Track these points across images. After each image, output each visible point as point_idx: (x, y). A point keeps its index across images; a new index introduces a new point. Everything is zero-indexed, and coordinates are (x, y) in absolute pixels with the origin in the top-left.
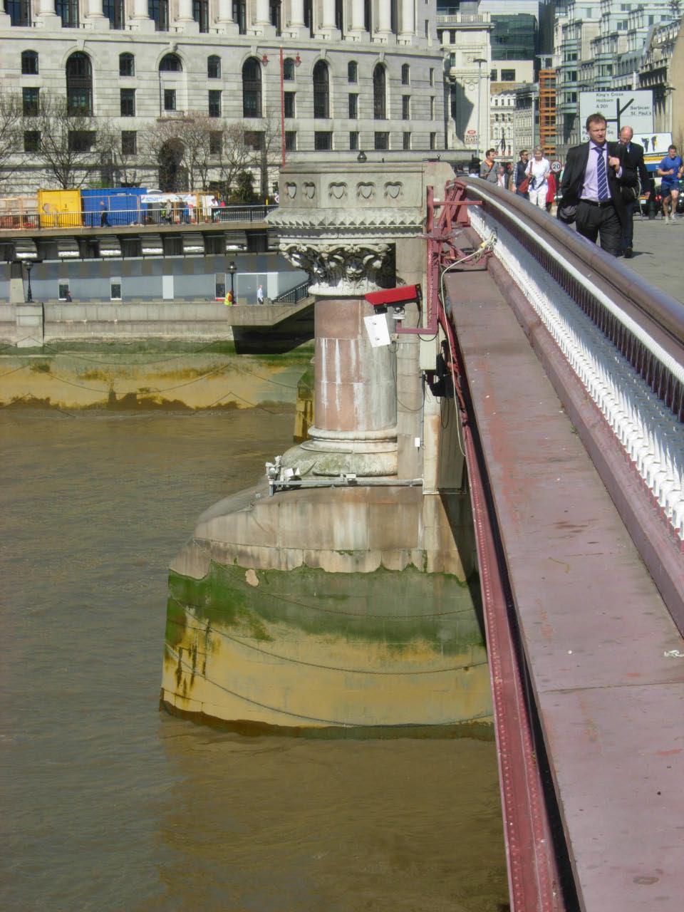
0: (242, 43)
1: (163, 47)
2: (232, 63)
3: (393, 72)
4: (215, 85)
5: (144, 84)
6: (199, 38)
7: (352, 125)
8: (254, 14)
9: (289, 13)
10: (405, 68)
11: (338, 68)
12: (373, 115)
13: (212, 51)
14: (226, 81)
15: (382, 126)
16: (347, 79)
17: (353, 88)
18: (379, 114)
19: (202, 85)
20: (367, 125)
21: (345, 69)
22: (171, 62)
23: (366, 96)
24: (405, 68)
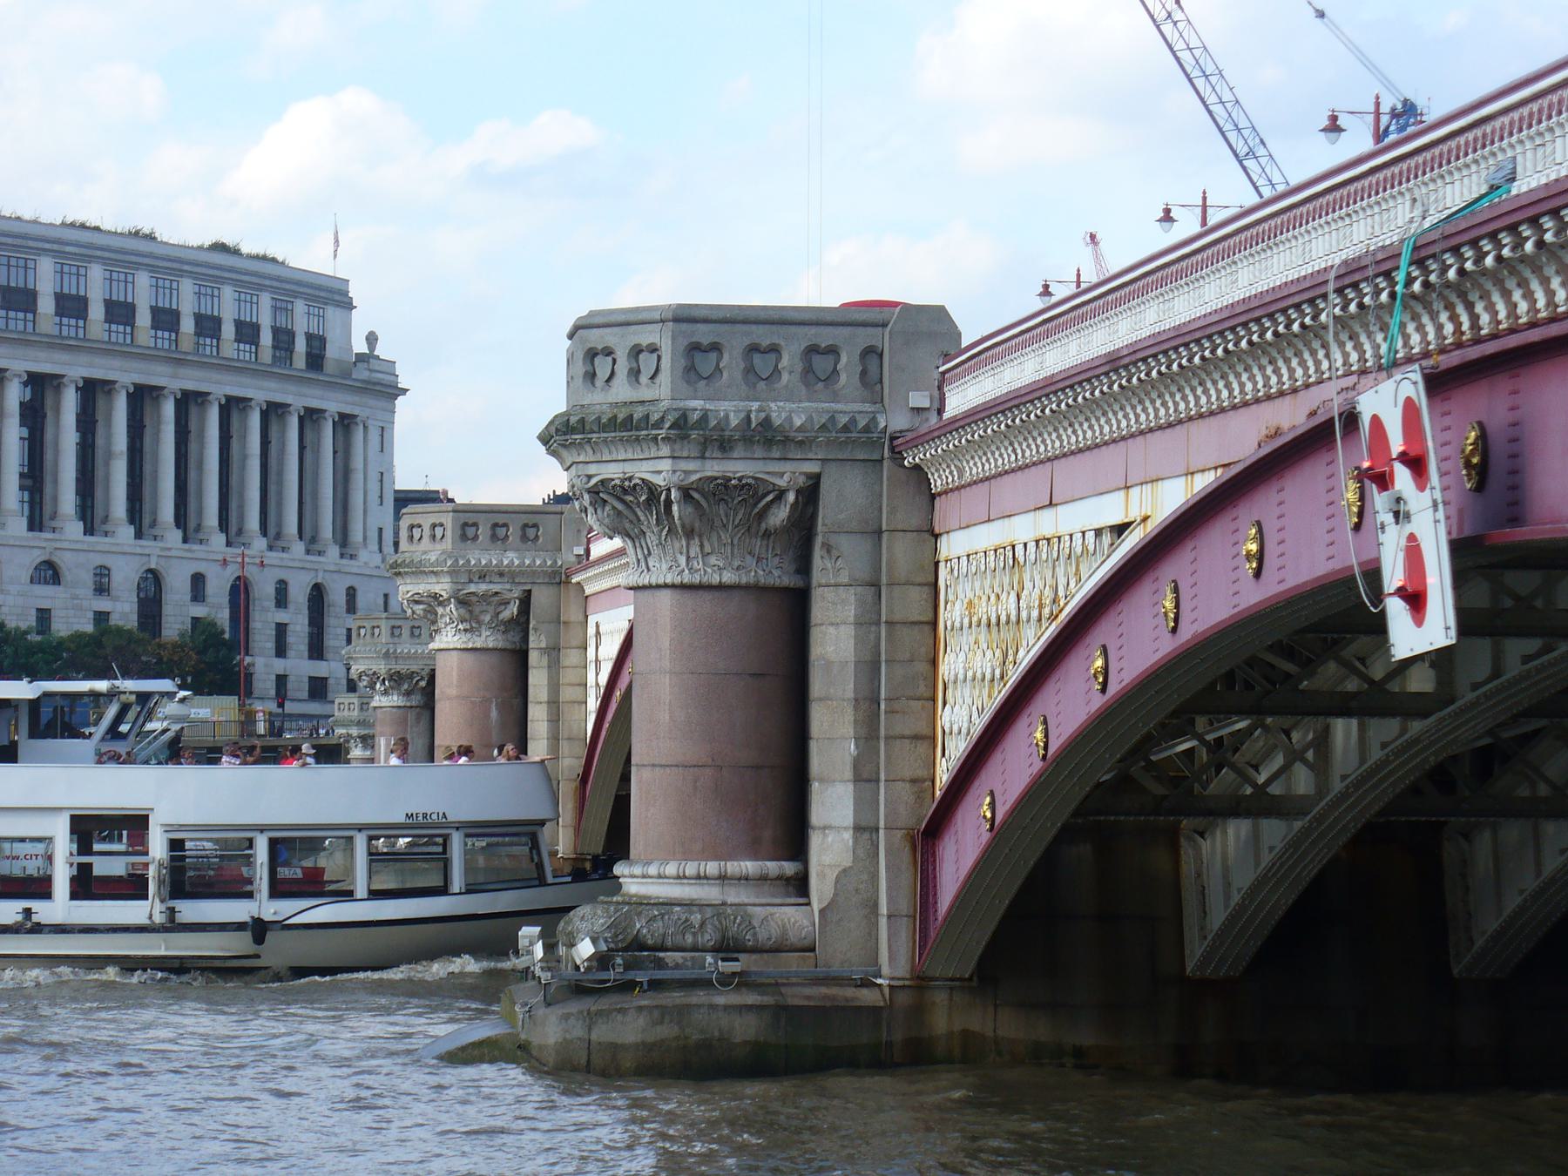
0: (138, 550)
1: (36, 552)
2: (125, 576)
3: (336, 597)
4: (103, 605)
5: (10, 600)
6: (83, 542)
7: (279, 666)
8: (154, 512)
9: (200, 512)
10: (351, 593)
11: (264, 589)
12: (306, 654)
13: (99, 560)
14: (116, 599)
15: (320, 669)
16: (273, 603)
17: (282, 616)
18: (317, 650)
19: (85, 603)
20: (300, 667)
21: (270, 590)
22: (49, 573)
23: (298, 628)
24: (351, 593)
